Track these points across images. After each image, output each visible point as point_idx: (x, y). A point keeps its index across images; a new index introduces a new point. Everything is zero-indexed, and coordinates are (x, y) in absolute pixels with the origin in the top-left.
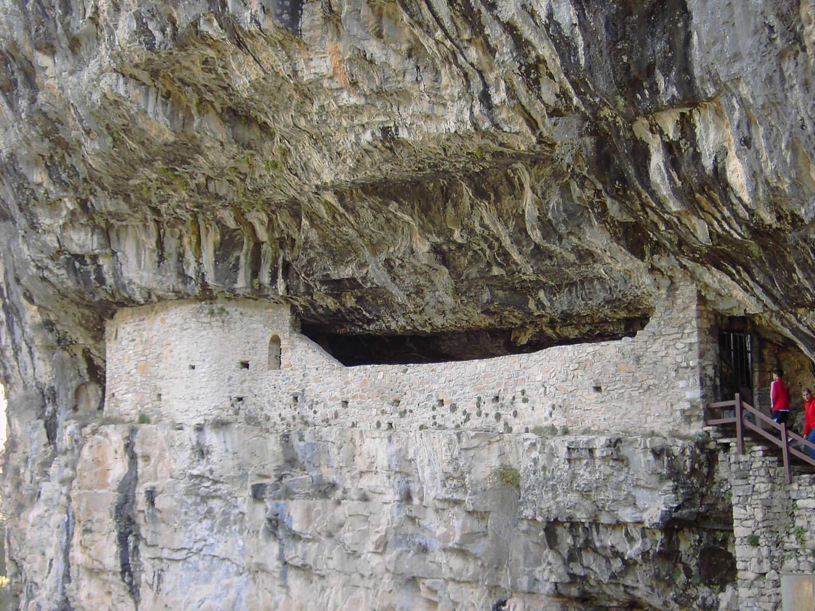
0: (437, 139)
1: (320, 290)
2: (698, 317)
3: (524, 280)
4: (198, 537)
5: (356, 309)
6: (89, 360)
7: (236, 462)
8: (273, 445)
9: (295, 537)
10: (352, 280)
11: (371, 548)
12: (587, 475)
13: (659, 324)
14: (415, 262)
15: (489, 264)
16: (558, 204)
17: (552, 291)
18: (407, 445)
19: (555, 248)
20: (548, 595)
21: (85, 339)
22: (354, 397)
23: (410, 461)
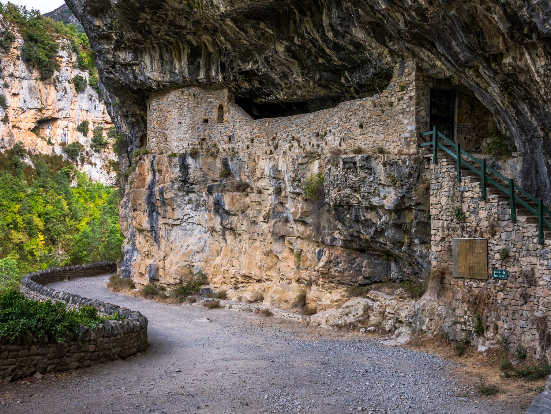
1: (240, 78)
2: (416, 80)
3: (336, 65)
4: (185, 213)
5: (260, 88)
7: (202, 173)
8: (218, 164)
9: (228, 213)
10: (252, 70)
11: (262, 219)
12: (354, 177)
13: (394, 85)
14: (278, 57)
15: (317, 58)
16: (335, 13)
17: (352, 71)
18: (278, 162)
19: (341, 42)
20: (341, 247)
21: (140, 111)
22: (256, 137)
23: (280, 171)
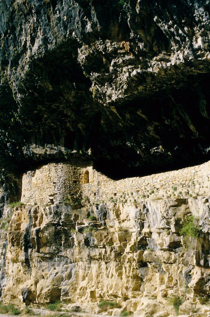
0: (166, 70)
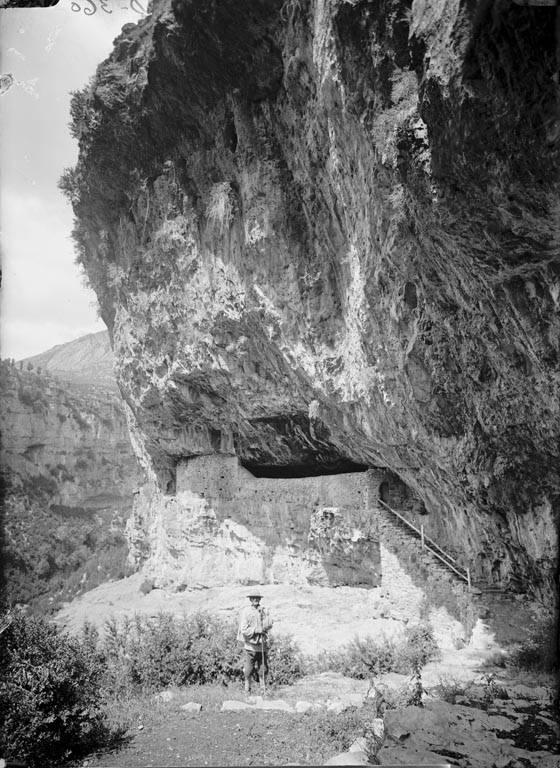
6: (171, 473)
